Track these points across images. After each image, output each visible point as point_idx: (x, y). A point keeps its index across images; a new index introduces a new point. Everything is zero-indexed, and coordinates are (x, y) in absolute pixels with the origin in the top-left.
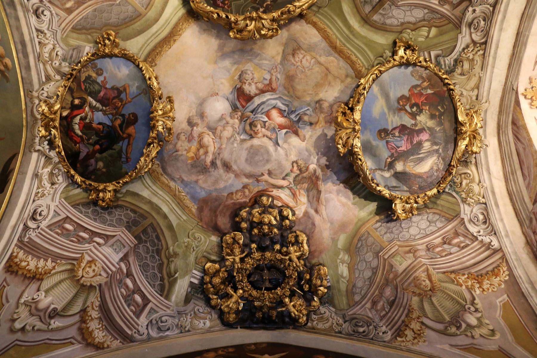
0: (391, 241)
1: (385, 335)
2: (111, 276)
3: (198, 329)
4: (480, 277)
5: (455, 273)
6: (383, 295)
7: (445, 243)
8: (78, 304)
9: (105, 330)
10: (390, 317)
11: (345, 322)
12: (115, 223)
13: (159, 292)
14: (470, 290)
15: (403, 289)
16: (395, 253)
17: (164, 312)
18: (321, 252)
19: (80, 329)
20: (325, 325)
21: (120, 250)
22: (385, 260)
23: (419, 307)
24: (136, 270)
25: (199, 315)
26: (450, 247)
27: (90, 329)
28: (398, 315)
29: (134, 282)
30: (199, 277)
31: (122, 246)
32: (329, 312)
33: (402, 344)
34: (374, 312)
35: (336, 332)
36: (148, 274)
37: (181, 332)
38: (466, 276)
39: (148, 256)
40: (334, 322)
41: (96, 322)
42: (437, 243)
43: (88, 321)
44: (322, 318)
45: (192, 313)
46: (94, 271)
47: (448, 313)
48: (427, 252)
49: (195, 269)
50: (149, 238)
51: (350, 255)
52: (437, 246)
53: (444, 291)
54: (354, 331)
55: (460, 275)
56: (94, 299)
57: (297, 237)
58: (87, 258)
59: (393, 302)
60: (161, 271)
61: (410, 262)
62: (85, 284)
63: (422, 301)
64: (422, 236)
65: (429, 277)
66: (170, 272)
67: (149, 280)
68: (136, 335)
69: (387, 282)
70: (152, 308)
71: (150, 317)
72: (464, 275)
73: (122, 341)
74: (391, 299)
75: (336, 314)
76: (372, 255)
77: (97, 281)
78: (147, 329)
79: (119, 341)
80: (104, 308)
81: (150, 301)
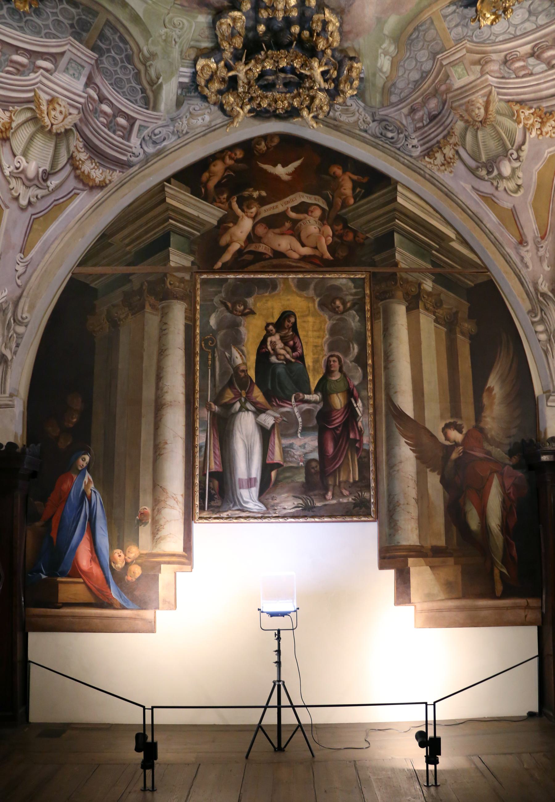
0: (458, 41)
1: (414, 149)
2: (83, 110)
3: (197, 128)
4: (548, 115)
5: (521, 105)
6: (427, 105)
7: (532, 55)
8: (62, 154)
9: (100, 167)
10: (426, 132)
11: (374, 121)
12: (54, 32)
13: (145, 106)
14: (526, 129)
15: (451, 108)
16: (458, 61)
17: (155, 125)
18: (357, 35)
19: (77, 177)
20: (350, 119)
21: (80, 74)
22: (442, 66)
23: (461, 133)
24: (108, 91)
25: (196, 114)
26: (538, 62)
27: (86, 172)
28: (435, 133)
29: (111, 105)
30: (189, 74)
31: (80, 68)
32: (357, 106)
33: (428, 166)
34: (409, 119)
35: (360, 130)
36: (125, 90)
37: (179, 137)
38: (532, 111)
39: (118, 69)
40: (361, 117)
41: (88, 163)
42: (522, 53)
43: (80, 166)
44: (347, 110)
45: (188, 114)
46: (61, 112)
47: (487, 154)
48: (502, 67)
49: (183, 66)
50: (110, 44)
51: (398, 47)
52: (519, 59)
53: (495, 128)
54: (381, 134)
55: (527, 107)
56: (76, 142)
57: (325, 23)
58: (44, 98)
59: (435, 117)
60: (140, 83)
61: (472, 78)
62: (59, 131)
63: (466, 129)
64: (507, 36)
65: (487, 105)
66: (151, 80)
67: (129, 97)
68: (133, 159)
69: (435, 93)
70: (140, 126)
71: (141, 135)
72: (531, 108)
73: (121, 170)
74: (434, 113)
75: (364, 109)
76: (427, 54)
77: (70, 122)
78: (142, 147)
79: (118, 171)
80: (90, 146)
81: (135, 119)
